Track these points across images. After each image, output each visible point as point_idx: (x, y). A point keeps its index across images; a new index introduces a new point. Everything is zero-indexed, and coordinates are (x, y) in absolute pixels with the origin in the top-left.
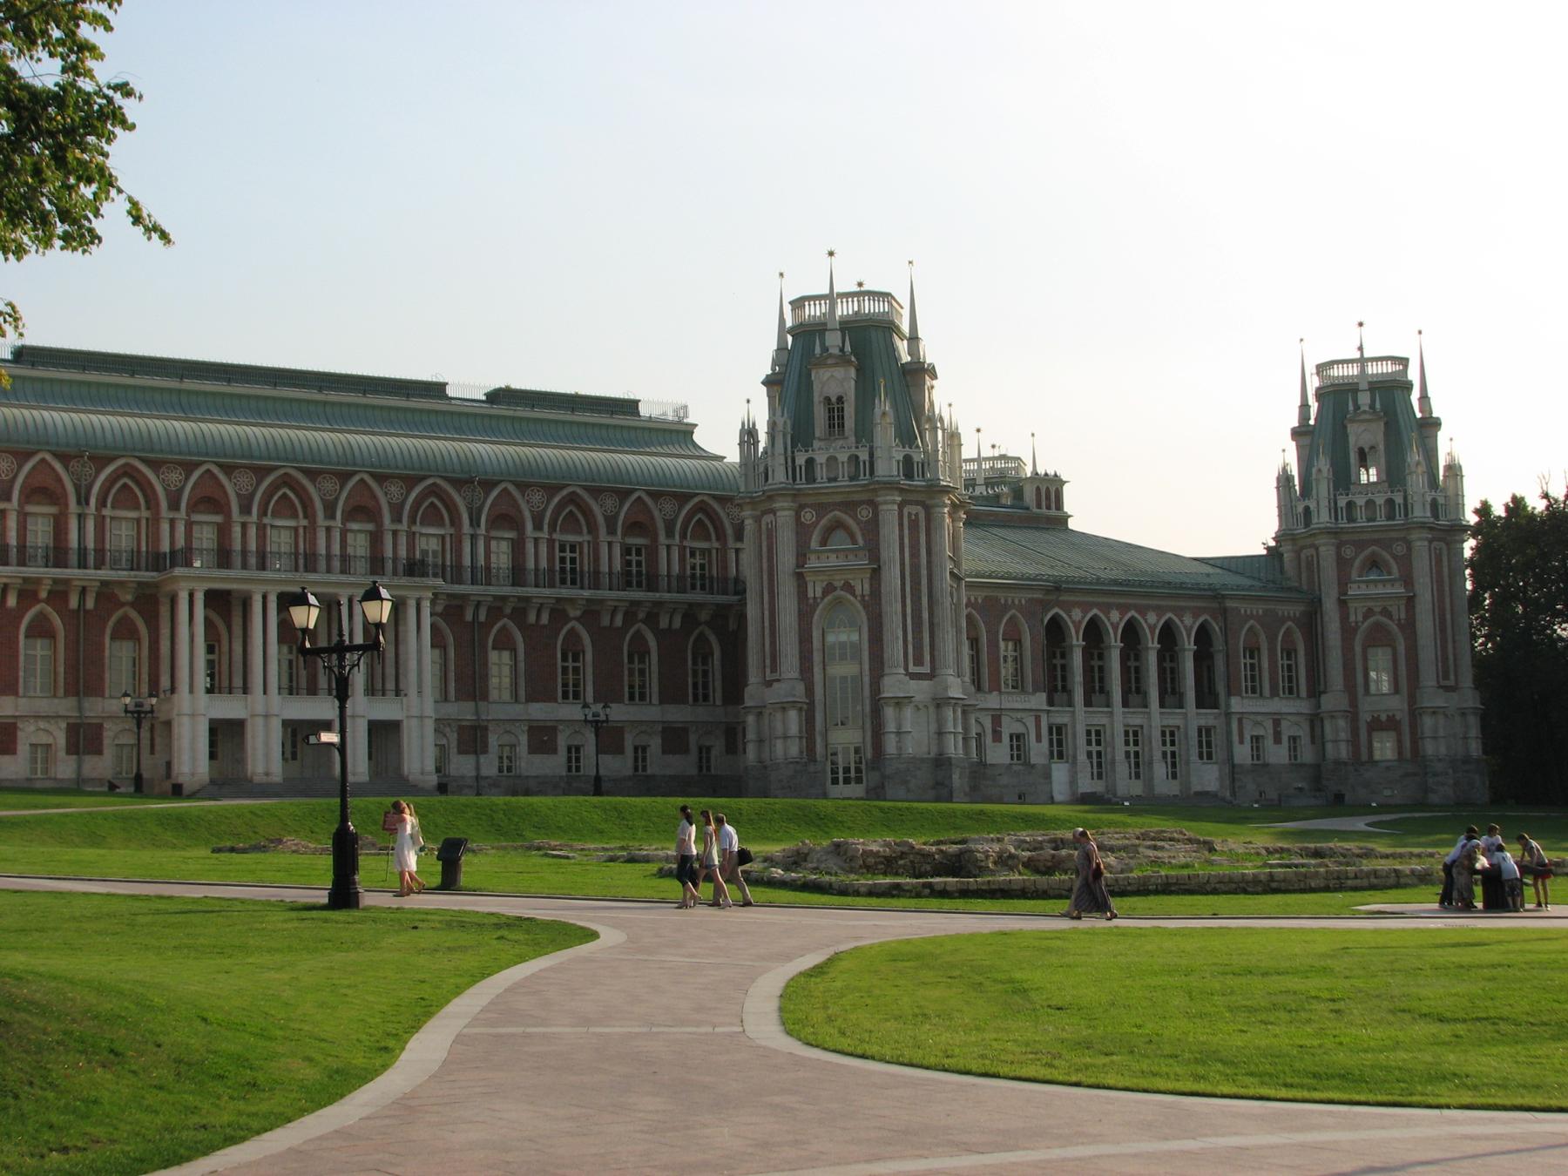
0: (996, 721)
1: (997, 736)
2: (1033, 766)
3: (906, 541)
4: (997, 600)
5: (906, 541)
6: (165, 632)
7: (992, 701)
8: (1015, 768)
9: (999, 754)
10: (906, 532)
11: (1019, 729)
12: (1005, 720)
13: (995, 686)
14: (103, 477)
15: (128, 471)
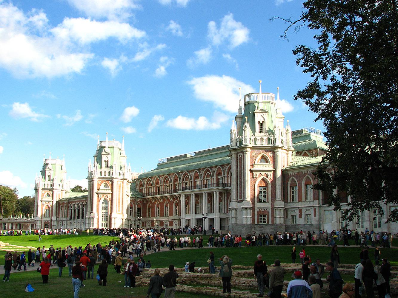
0: (300, 210)
1: (300, 216)
2: (312, 225)
3: (238, 164)
4: (302, 172)
5: (238, 164)
6: (212, 201)
7: (300, 205)
8: (306, 225)
9: (300, 221)
10: (238, 161)
11: (307, 213)
12: (303, 211)
13: (300, 200)
14: (182, 176)
15: (186, 174)
